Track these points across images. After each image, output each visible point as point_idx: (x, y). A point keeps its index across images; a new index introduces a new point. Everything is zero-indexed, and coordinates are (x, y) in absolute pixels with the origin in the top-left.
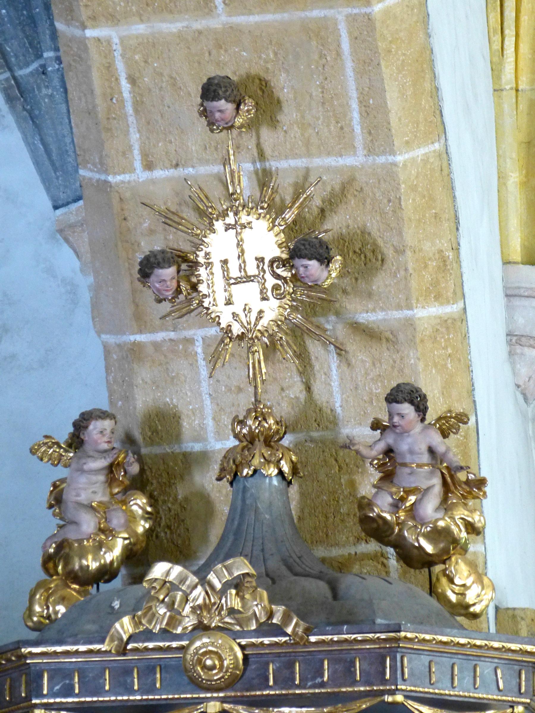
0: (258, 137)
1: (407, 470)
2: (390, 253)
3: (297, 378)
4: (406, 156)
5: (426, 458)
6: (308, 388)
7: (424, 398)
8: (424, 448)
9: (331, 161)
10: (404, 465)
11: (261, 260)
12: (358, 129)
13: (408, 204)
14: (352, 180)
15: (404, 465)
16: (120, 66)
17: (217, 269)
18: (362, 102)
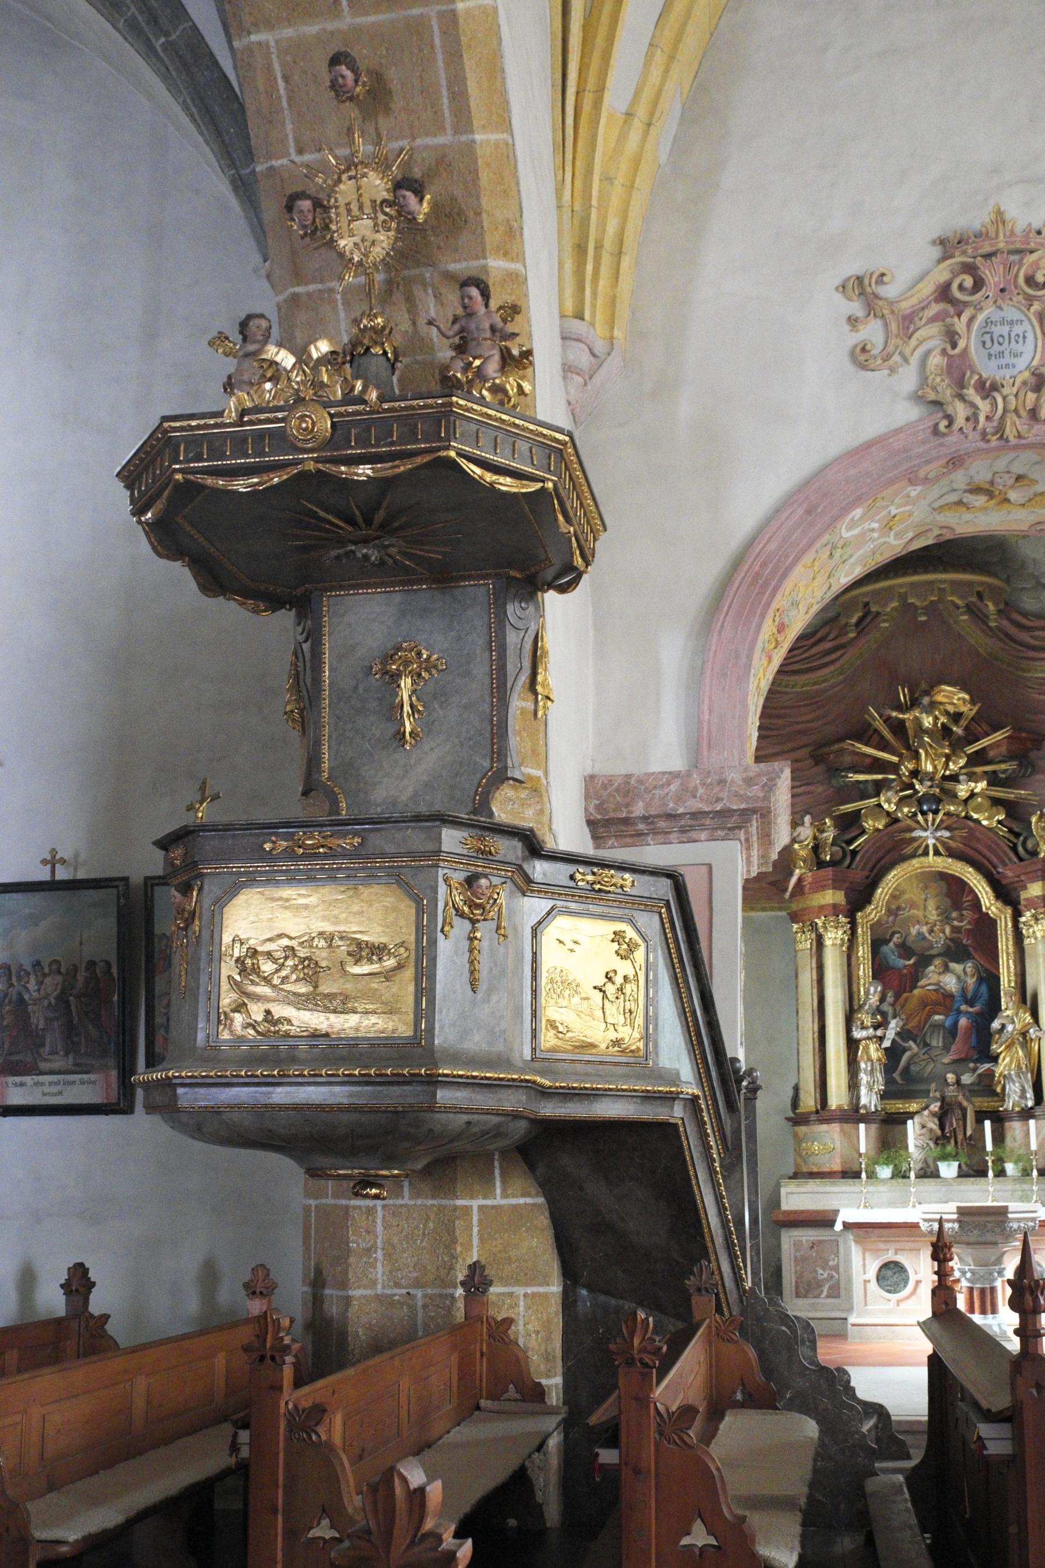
0: (376, 123)
1: (474, 343)
2: (471, 214)
3: (406, 316)
5: (488, 334)
6: (414, 323)
7: (487, 287)
8: (487, 326)
9: (429, 141)
10: (473, 339)
11: (374, 202)
14: (444, 156)
15: (473, 339)
16: (277, 66)
17: (342, 210)
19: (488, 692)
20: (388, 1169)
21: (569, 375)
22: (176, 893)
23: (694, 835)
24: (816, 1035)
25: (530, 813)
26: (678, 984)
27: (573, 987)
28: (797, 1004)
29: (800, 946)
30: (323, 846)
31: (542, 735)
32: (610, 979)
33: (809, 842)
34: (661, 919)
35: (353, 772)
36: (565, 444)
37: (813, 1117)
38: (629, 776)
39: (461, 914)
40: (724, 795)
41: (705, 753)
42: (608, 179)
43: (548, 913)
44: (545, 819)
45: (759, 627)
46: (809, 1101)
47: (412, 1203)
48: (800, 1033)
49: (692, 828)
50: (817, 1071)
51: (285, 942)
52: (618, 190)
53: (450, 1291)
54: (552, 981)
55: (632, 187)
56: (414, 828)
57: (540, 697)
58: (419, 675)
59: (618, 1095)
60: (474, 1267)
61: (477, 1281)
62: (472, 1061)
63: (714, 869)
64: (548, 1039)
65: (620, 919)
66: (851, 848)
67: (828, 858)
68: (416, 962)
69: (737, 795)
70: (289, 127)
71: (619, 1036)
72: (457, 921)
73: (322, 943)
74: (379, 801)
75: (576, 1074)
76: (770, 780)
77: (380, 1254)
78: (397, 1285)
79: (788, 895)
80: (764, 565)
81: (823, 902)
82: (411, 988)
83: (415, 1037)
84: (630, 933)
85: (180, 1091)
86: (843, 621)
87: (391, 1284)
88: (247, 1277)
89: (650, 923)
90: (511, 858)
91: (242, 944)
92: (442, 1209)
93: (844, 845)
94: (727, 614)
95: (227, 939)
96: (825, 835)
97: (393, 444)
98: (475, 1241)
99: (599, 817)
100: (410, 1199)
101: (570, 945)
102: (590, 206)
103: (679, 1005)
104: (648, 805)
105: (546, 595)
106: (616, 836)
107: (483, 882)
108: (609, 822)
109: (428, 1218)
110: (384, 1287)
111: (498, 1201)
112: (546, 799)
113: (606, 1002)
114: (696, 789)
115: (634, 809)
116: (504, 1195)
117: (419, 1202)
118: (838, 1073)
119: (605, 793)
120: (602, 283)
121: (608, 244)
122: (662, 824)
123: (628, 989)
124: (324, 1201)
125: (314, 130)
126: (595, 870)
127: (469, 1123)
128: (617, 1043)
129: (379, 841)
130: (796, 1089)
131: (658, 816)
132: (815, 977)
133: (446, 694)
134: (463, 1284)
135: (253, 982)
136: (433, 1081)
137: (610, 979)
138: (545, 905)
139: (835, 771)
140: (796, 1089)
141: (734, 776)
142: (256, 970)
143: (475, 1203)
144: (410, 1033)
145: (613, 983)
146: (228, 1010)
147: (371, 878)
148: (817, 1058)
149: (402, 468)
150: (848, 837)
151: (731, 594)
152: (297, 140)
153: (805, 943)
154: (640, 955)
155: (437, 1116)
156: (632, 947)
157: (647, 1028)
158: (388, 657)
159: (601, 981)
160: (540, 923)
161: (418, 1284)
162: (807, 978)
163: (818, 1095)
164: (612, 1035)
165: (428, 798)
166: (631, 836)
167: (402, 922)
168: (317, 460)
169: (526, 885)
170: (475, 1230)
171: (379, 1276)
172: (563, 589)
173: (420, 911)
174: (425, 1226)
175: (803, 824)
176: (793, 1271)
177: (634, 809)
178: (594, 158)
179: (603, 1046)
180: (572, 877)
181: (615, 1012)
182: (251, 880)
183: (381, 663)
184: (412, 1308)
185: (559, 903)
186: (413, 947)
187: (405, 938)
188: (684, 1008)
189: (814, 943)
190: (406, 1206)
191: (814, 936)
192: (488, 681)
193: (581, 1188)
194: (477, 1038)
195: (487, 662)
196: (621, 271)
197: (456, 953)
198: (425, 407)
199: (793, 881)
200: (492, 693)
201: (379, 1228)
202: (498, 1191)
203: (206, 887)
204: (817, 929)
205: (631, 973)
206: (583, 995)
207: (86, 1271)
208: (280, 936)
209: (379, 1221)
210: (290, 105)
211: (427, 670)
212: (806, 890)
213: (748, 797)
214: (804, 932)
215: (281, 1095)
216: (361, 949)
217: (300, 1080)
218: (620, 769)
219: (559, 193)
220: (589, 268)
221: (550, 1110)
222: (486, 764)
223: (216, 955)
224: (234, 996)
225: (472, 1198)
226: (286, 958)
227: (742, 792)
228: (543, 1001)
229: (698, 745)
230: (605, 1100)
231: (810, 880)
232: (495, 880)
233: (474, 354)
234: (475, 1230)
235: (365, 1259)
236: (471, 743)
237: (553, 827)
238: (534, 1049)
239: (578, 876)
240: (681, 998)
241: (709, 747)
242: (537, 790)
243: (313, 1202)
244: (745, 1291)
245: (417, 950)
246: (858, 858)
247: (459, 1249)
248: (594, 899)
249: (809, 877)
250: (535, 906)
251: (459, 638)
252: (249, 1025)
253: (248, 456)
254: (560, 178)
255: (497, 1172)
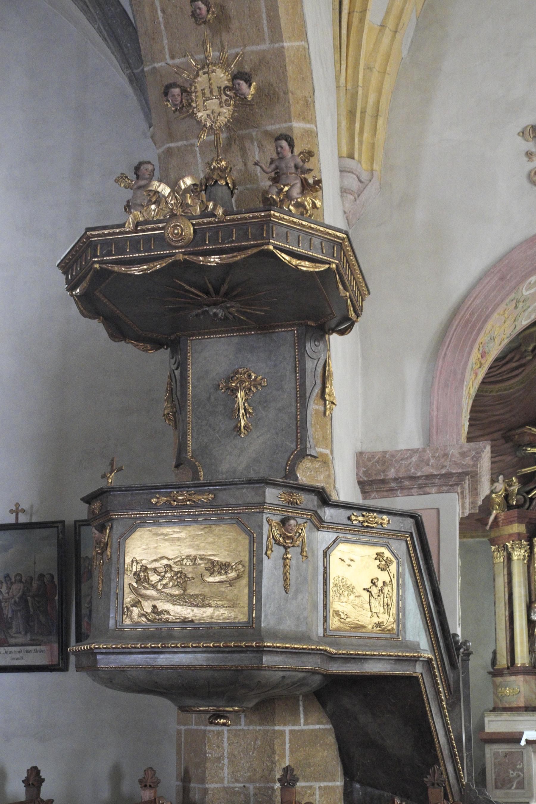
1: (284, 176)
3: (240, 160)
4: (289, 44)
5: (293, 170)
6: (245, 165)
8: (292, 165)
9: (255, 48)
12: (266, 29)
13: (290, 68)
17: (200, 94)
18: (268, 14)
19: (294, 400)
20: (232, 707)
21: (345, 194)
22: (96, 531)
23: (427, 490)
24: (507, 618)
25: (321, 477)
26: (418, 586)
27: (351, 589)
28: (495, 599)
29: (497, 561)
30: (189, 500)
31: (329, 427)
32: (374, 584)
33: (502, 493)
34: (407, 544)
35: (208, 452)
36: (343, 239)
37: (506, 672)
38: (385, 452)
39: (278, 543)
40: (447, 463)
41: (435, 437)
42: (369, 68)
43: (334, 542)
44: (331, 481)
45: (469, 353)
46: (503, 661)
47: (246, 728)
48: (497, 616)
49: (426, 485)
50: (508, 641)
51: (165, 562)
52: (375, 77)
53: (272, 785)
54: (336, 585)
55: (385, 72)
56: (247, 488)
57: (327, 402)
58: (250, 389)
59: (379, 658)
60: (287, 770)
61: (289, 779)
62: (286, 638)
63: (441, 511)
64: (334, 623)
65: (381, 545)
66: (530, 496)
67: (514, 503)
68: (250, 573)
69: (455, 463)
70: (165, 42)
71: (380, 620)
72: (275, 547)
73: (189, 562)
74: (224, 470)
75: (352, 645)
76: (477, 453)
77: (226, 761)
78: (237, 781)
79: (488, 527)
80: (472, 314)
81: (511, 532)
82: (246, 591)
83: (248, 622)
84: (387, 554)
85: (99, 657)
86: (523, 349)
87: (234, 780)
88: (141, 775)
89: (400, 547)
90: (310, 506)
91: (138, 563)
92: (266, 732)
93: (525, 494)
94: (448, 347)
95: (128, 560)
96: (512, 488)
97: (233, 242)
98: (287, 753)
99: (366, 479)
100: (245, 725)
101: (348, 562)
102: (358, 86)
103: (419, 600)
104: (397, 471)
105: (331, 337)
106: (377, 491)
107: (292, 522)
108: (372, 482)
109: (256, 739)
110: (228, 782)
111: (302, 727)
112: (331, 468)
113: (372, 598)
114: (429, 460)
115: (388, 473)
116: (306, 723)
117: (251, 728)
118: (522, 643)
119: (370, 464)
120: (366, 135)
121: (369, 111)
122: (407, 483)
123: (386, 590)
124: (190, 727)
125: (182, 43)
126: (364, 513)
127: (284, 677)
128: (378, 625)
129: (224, 497)
130: (495, 653)
131: (403, 478)
132: (506, 581)
133: (266, 401)
134: (279, 780)
135: (145, 588)
136: (260, 651)
137: (374, 584)
138: (332, 536)
139: (519, 446)
140: (495, 653)
141: (454, 451)
142: (147, 580)
143: (287, 729)
144: (245, 620)
145: (376, 586)
146: (129, 605)
147: (220, 520)
148: (508, 632)
149: (239, 257)
150: (528, 489)
151: (451, 333)
152: (171, 51)
153: (500, 558)
154: (393, 568)
155: (263, 673)
156: (388, 563)
157: (398, 615)
158: (229, 379)
159: (368, 585)
160: (328, 548)
161: (250, 780)
162: (501, 581)
163: (509, 658)
164: (376, 620)
165: (256, 468)
166: (387, 491)
167: (240, 548)
168: (184, 253)
169: (320, 524)
170: (287, 746)
171: (226, 775)
172: (342, 333)
173: (251, 542)
174: (255, 743)
175: (498, 481)
176: (493, 771)
177: (388, 473)
178: (360, 55)
179: (370, 627)
180: (349, 518)
181: (377, 604)
182: (143, 522)
183: (225, 382)
184: (247, 796)
185: (341, 535)
186: (247, 564)
187: (242, 558)
188: (422, 602)
189: (506, 558)
190: (243, 730)
191: (505, 554)
192: (294, 392)
193: (356, 719)
194: (288, 622)
195: (293, 381)
196: (378, 127)
197: (275, 568)
198: (253, 218)
199: (492, 518)
200: (297, 400)
201: (226, 745)
202: (302, 721)
203: (115, 527)
204: (507, 549)
205: (388, 580)
206: (357, 594)
207: (38, 772)
208: (162, 558)
209: (225, 740)
210: (165, 27)
211: (255, 386)
212: (500, 524)
213: (463, 464)
214: (499, 551)
215: (163, 660)
216: (214, 566)
217: (175, 650)
218: (380, 448)
219: (337, 79)
220: (357, 125)
221: (336, 668)
222: (293, 446)
223: (121, 571)
224: (133, 596)
225: (285, 725)
226: (166, 572)
227: (459, 461)
228: (331, 598)
229: (429, 432)
230: (371, 662)
231: (503, 517)
232: (300, 521)
233: (284, 183)
234: (287, 746)
235: (216, 764)
236: (284, 432)
237: (336, 486)
238: (325, 630)
239: (353, 518)
240: (420, 596)
241: (437, 432)
242: (326, 463)
243: (183, 728)
244: (463, 785)
245: (250, 566)
246: (534, 503)
247: (277, 758)
248: (363, 533)
249: (502, 516)
250: (325, 537)
251: (275, 366)
252: (143, 615)
253: (139, 251)
254: (338, 68)
255: (301, 708)
